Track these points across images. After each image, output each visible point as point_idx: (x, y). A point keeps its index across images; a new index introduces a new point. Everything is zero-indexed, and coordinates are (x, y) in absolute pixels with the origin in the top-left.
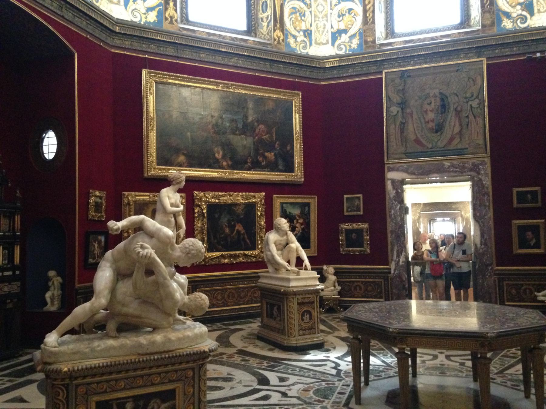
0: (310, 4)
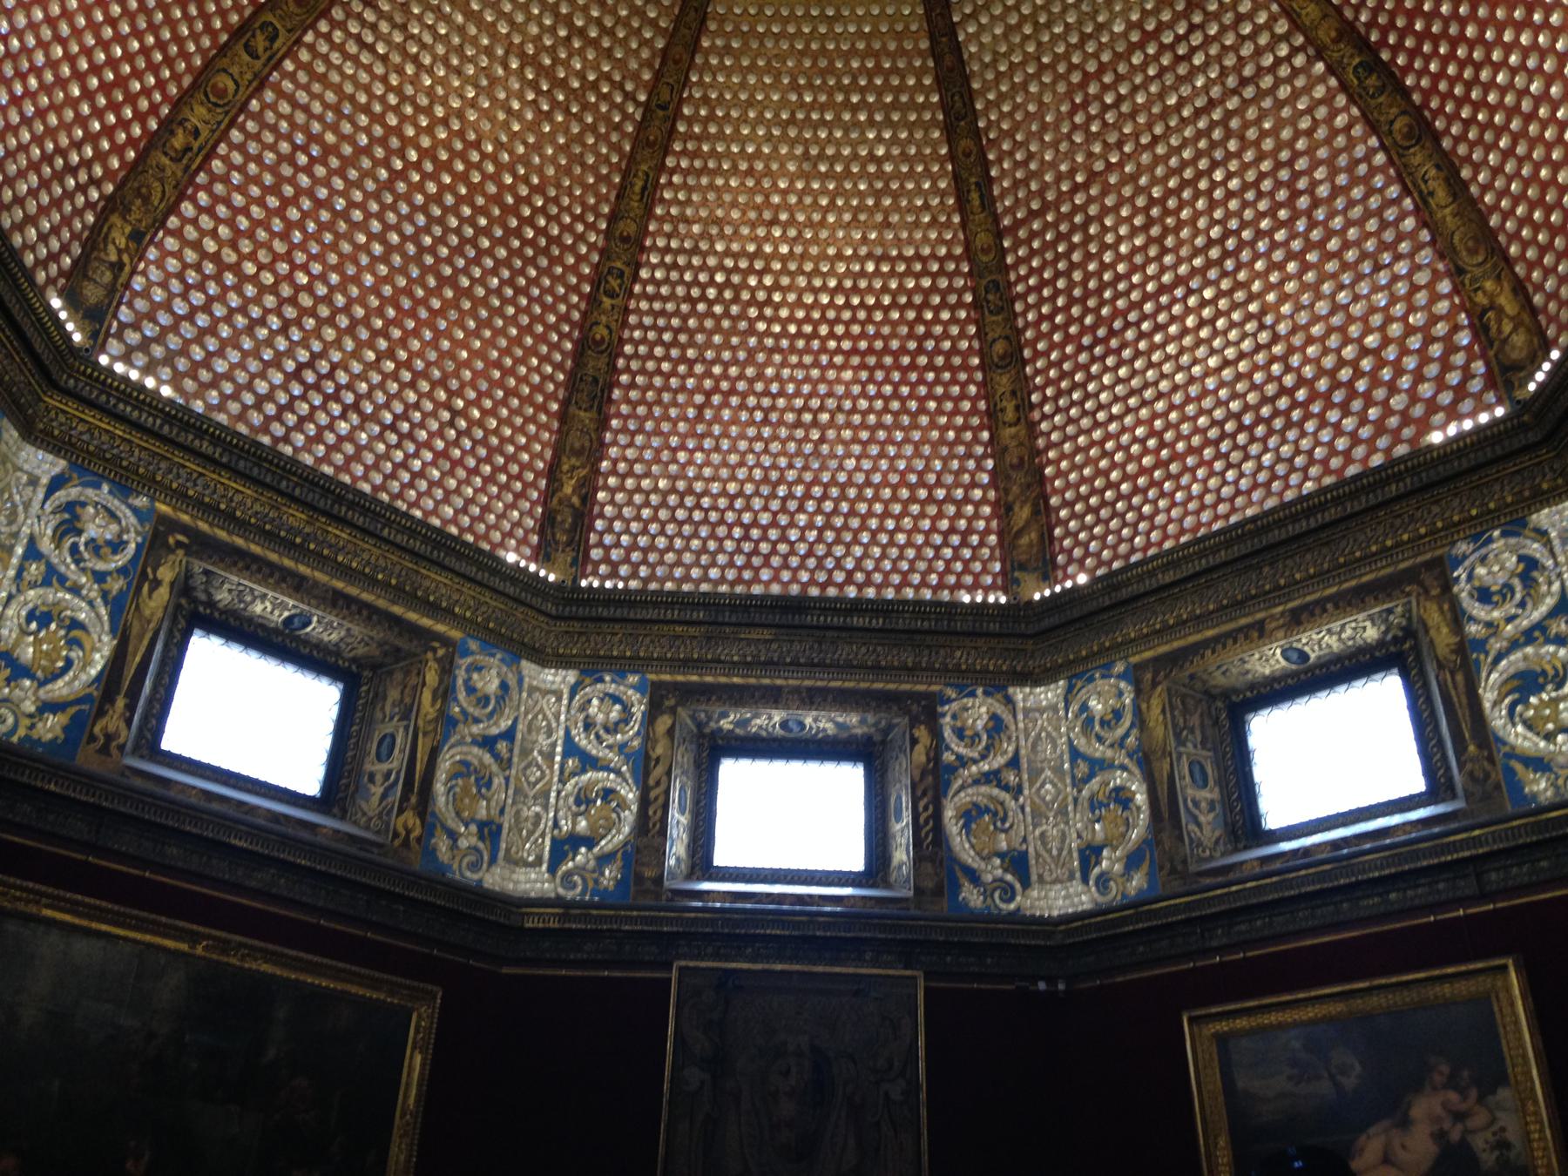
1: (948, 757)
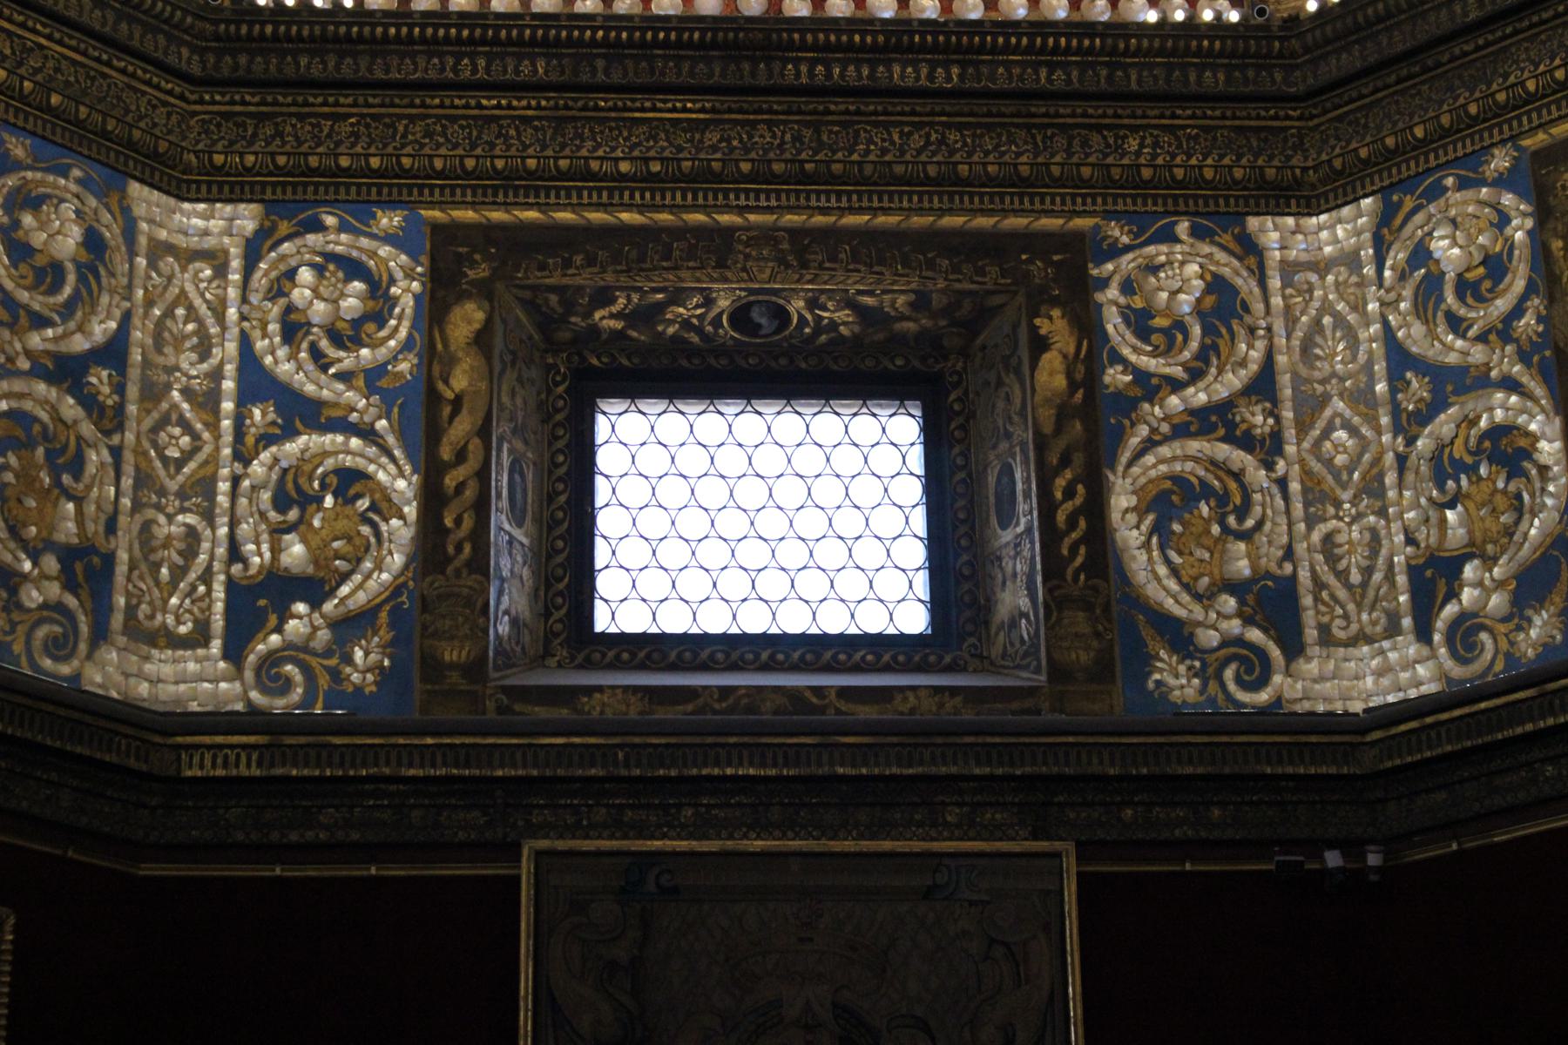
0: (120, 408)
1: (1116, 377)
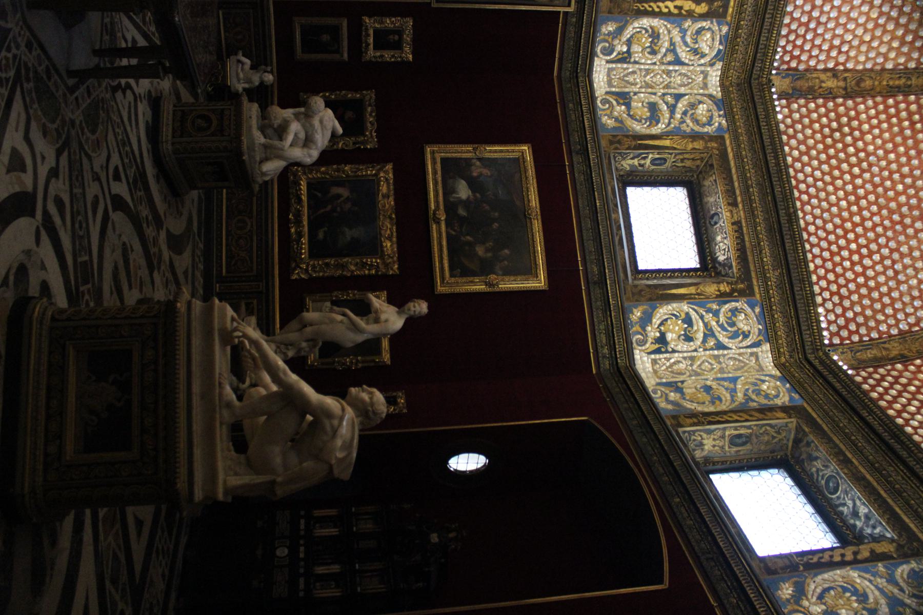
1: (687, 24)
